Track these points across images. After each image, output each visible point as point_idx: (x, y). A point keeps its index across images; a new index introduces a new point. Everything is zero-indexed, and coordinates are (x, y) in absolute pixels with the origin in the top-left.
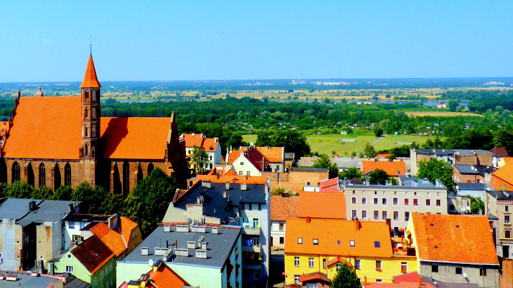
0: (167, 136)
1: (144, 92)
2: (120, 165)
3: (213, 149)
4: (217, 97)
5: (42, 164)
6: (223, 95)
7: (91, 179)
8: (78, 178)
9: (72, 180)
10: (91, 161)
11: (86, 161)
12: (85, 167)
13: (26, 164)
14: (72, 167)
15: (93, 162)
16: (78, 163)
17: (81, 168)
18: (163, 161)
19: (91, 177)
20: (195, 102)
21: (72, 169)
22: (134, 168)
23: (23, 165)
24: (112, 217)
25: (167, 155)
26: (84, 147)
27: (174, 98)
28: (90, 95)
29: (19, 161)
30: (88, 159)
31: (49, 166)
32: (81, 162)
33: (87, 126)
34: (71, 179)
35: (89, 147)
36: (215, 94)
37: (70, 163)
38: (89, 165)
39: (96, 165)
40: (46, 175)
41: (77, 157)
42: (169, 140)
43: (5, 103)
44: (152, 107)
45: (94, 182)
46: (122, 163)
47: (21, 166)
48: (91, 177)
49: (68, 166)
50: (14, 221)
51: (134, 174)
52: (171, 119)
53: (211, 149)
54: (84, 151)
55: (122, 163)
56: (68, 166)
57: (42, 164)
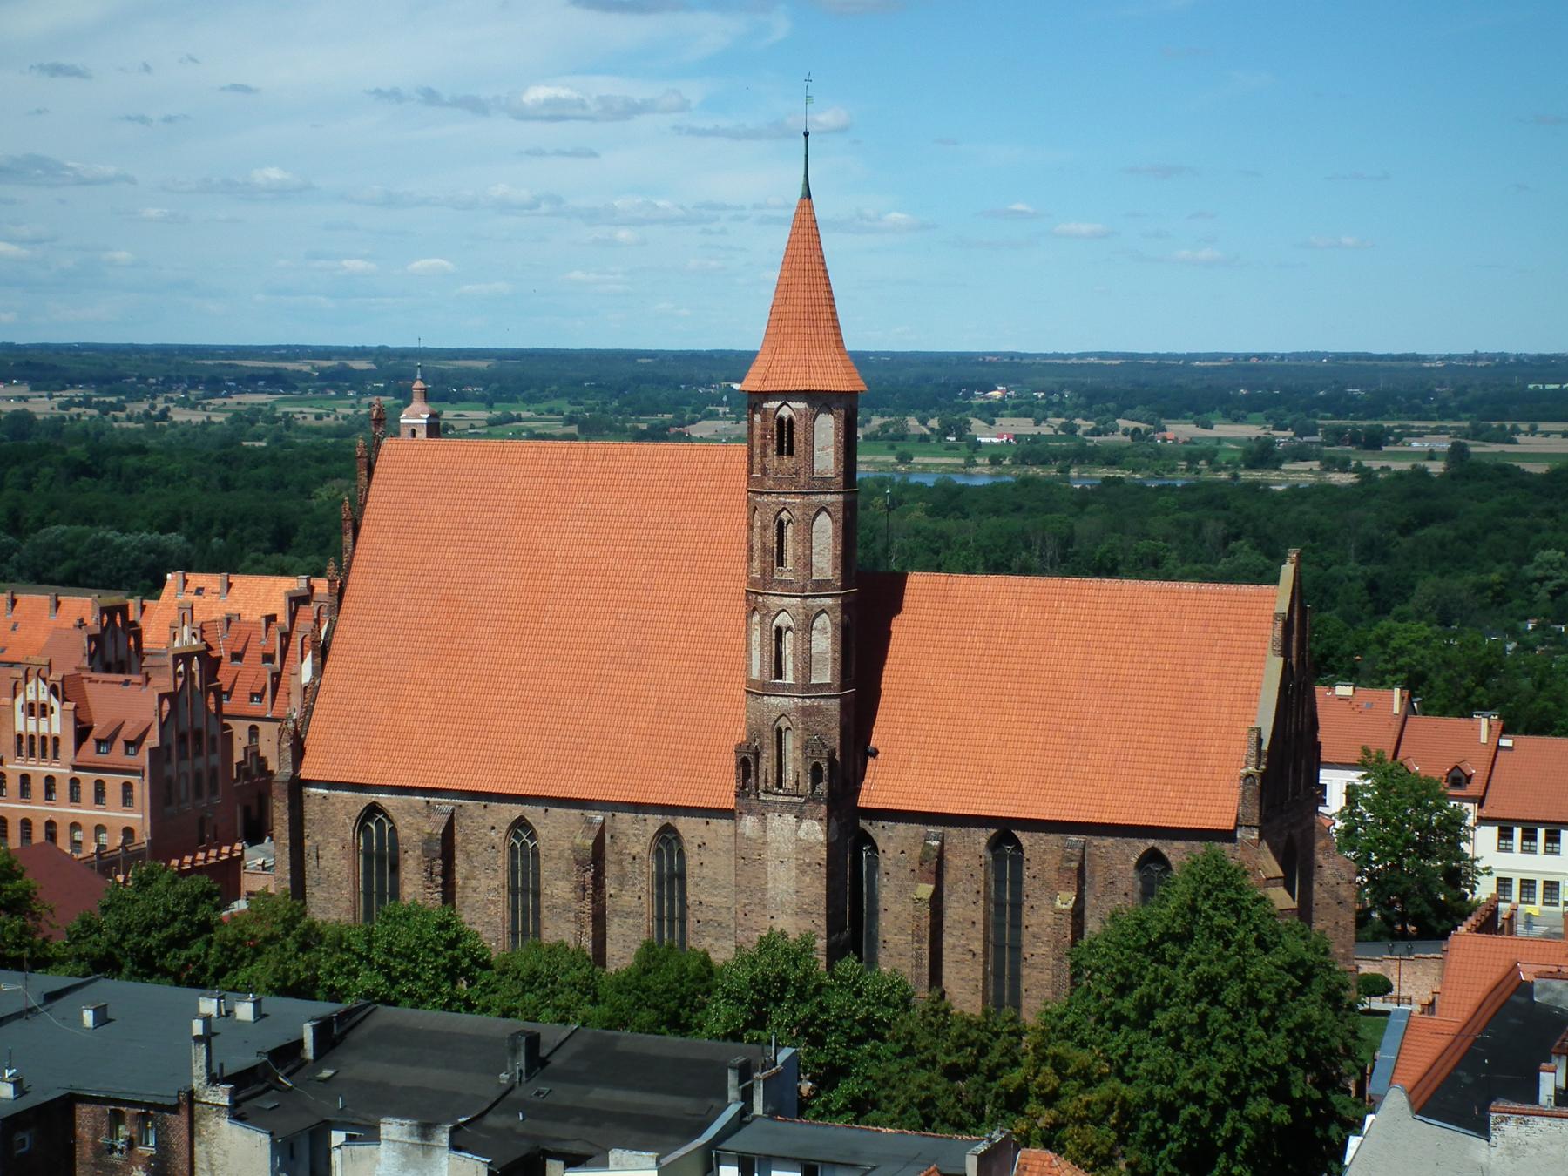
0: (1250, 697)
1: (934, 423)
2: (969, 852)
3: (1469, 778)
4: (1389, 463)
5: (520, 824)
6: (1425, 448)
7: (805, 924)
8: (725, 917)
9: (691, 925)
10: (806, 824)
11: (774, 821)
12: (770, 854)
13: (435, 827)
14: (690, 850)
15: (814, 831)
16: (722, 826)
17: (749, 857)
18: (1228, 836)
19: (802, 911)
20: (1253, 487)
21: (691, 863)
22: (1052, 875)
23: (413, 824)
24: (982, 1147)
25: (1254, 811)
26: (769, 739)
27: (1113, 458)
28: (799, 435)
29: (384, 799)
30: (789, 808)
31: (560, 835)
32: (749, 824)
33: (783, 620)
34: (683, 921)
35: (790, 743)
36: (1374, 441)
37: (682, 824)
38: (794, 838)
39: (830, 846)
40: (546, 890)
41: (724, 794)
42: (1265, 719)
43: (149, 461)
44: (997, 512)
45: (821, 943)
46: (982, 837)
47: (403, 833)
48: (802, 911)
49: (668, 840)
50: (443, 1137)
51: (1046, 909)
52: (1279, 597)
53: (1458, 778)
54: (767, 764)
55: (982, 837)
56: (668, 840)
57: (520, 824)
